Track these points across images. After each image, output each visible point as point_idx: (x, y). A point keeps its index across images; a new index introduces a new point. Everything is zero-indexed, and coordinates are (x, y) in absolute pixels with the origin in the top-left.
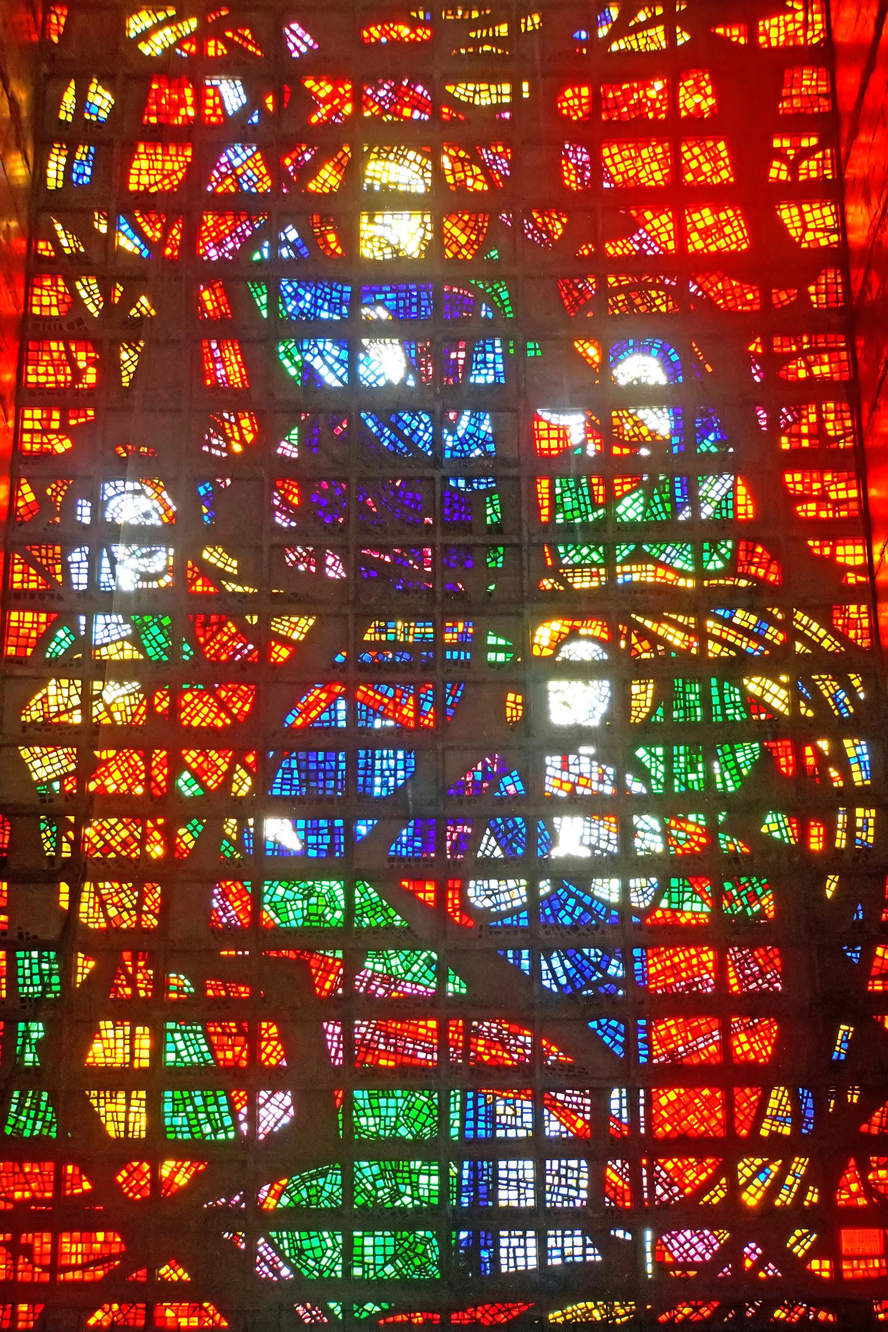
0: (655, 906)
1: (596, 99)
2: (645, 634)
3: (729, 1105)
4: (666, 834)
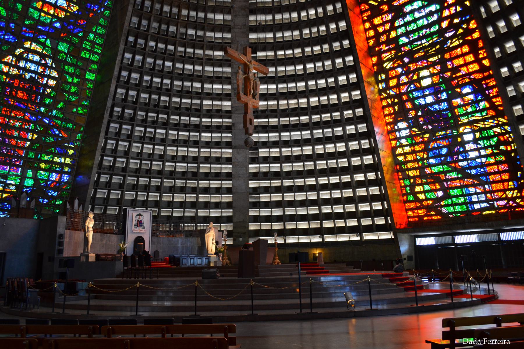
0: (486, 161)
1: (450, 55)
2: (476, 126)
3: (503, 185)
4: (485, 152)
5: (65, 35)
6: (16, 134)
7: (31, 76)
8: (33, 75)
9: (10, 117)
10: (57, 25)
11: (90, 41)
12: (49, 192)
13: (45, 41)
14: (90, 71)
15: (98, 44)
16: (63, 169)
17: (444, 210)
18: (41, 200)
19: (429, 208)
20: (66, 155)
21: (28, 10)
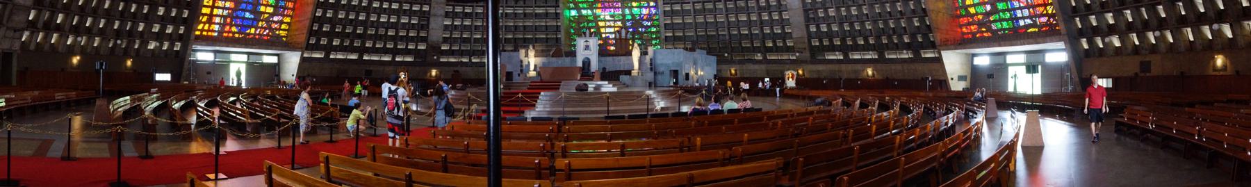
17: (994, 27)
18: (640, 29)
19: (980, 24)
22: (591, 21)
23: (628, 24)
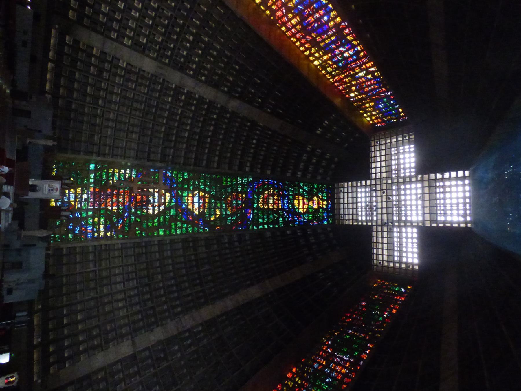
5: (180, 212)
6: (115, 200)
7: (151, 200)
8: (152, 201)
9: (124, 195)
10: (184, 206)
11: (182, 226)
12: (78, 228)
13: (173, 202)
14: (164, 231)
15: (182, 231)
16: (96, 232)
18: (71, 224)
20: (106, 232)
21: (186, 190)
22: (82, 181)
23: (77, 214)
